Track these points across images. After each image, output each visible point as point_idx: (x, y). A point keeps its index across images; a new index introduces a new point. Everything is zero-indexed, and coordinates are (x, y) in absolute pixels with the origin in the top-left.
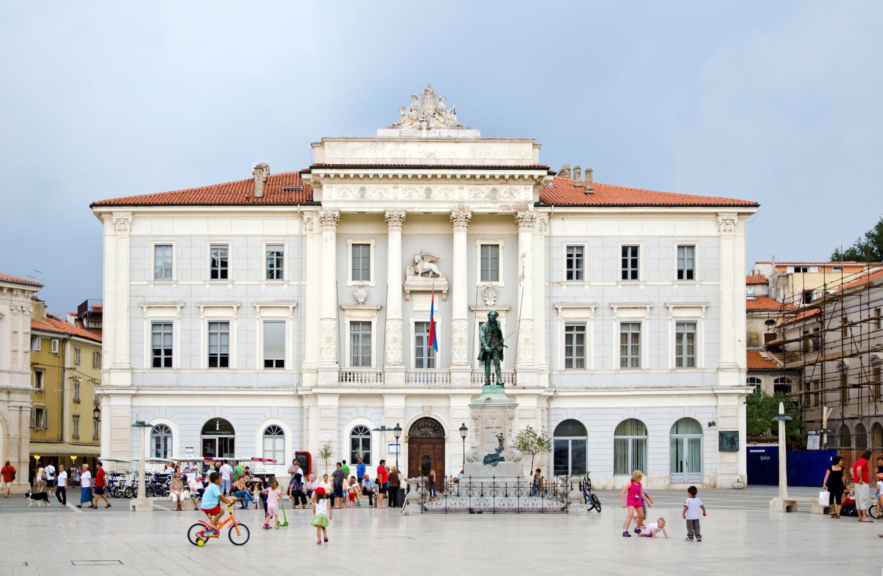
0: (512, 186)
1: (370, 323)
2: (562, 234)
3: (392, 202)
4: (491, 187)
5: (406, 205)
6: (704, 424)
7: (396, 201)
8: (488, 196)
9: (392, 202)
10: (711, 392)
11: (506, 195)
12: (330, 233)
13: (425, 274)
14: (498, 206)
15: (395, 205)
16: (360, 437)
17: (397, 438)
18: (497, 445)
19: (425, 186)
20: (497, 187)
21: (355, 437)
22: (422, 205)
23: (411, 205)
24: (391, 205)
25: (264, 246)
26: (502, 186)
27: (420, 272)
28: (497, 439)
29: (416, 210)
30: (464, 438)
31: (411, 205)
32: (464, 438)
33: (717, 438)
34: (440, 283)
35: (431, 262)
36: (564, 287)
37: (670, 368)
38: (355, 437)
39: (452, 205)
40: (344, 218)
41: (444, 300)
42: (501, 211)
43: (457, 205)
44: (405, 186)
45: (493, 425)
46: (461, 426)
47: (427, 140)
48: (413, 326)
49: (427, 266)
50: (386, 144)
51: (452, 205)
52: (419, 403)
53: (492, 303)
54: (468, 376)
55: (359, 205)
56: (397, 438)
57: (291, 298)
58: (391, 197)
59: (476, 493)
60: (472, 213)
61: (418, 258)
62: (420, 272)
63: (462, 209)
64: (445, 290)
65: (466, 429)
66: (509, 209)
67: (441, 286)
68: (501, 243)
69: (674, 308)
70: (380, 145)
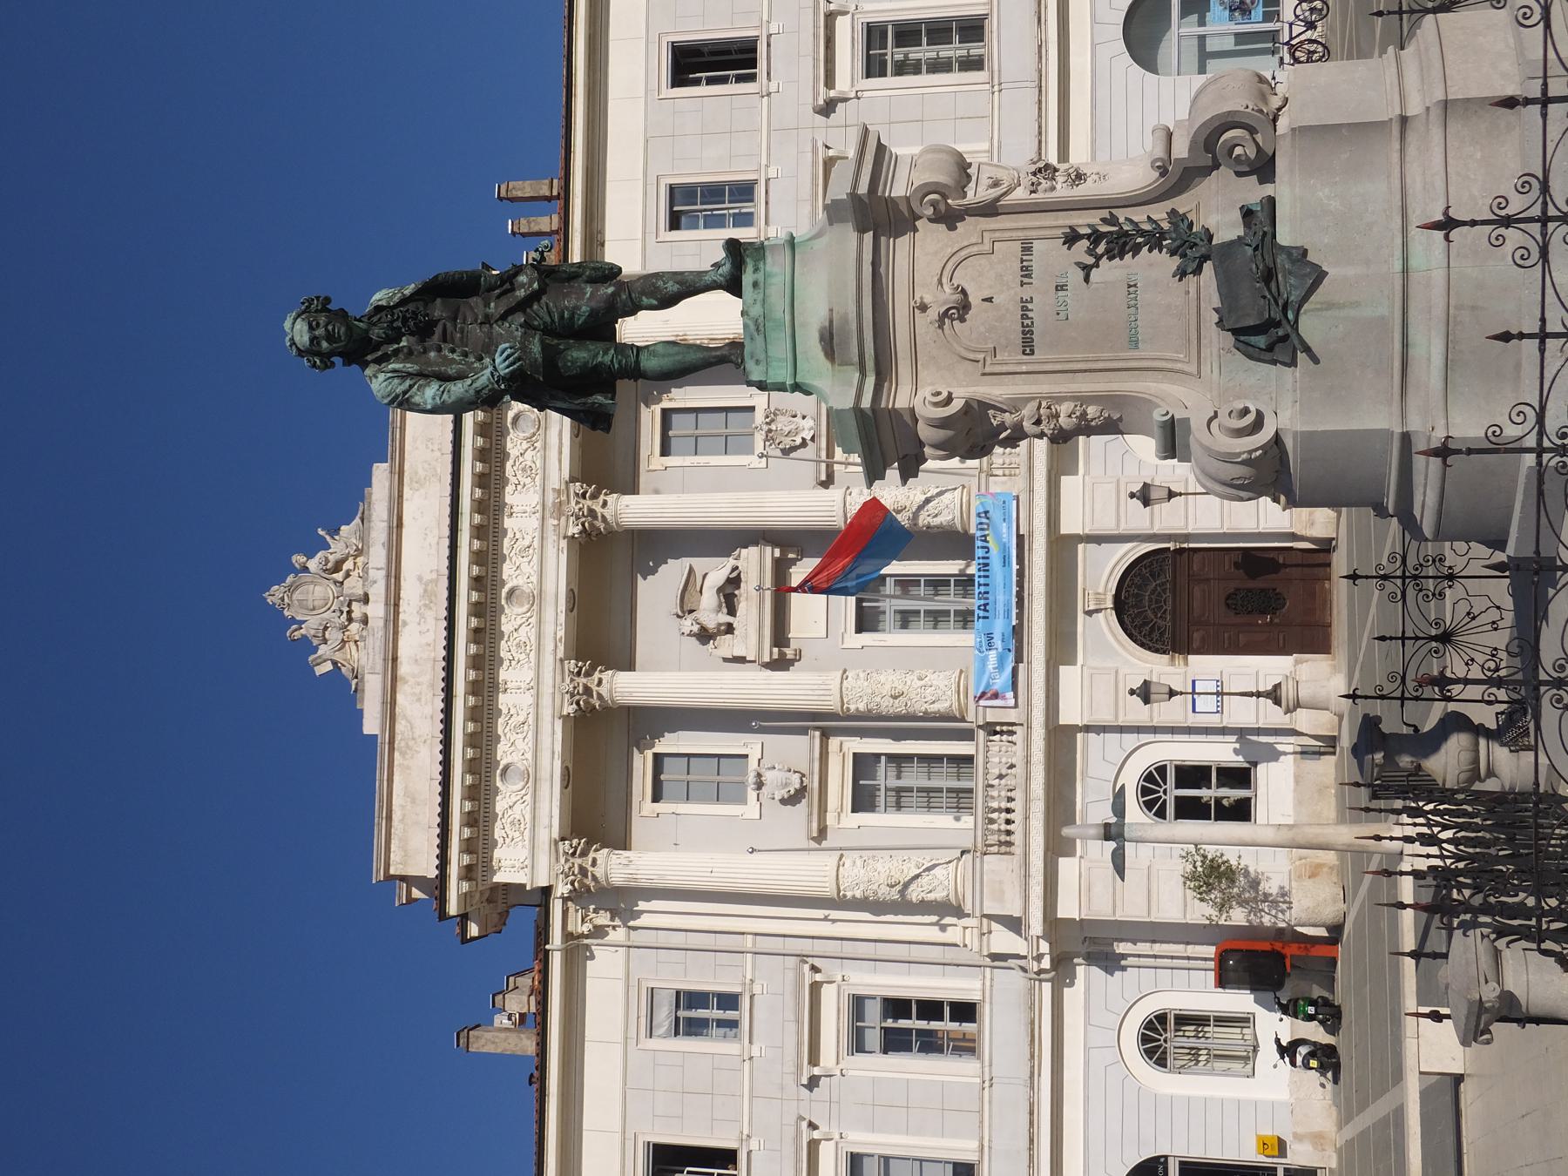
5: (548, 661)
15: (547, 688)
16: (1171, 792)
17: (1172, 693)
18: (1155, 266)
22: (549, 614)
23: (549, 646)
24: (546, 701)
25: (654, 1043)
27: (724, 618)
28: (1110, 271)
29: (561, 633)
30: (1171, 495)
31: (549, 646)
32: (1171, 495)
39: (551, 537)
45: (1007, 298)
46: (1137, 503)
48: (867, 638)
49: (709, 600)
51: (551, 537)
53: (809, 423)
55: (544, 789)
56: (1172, 693)
57: (790, 976)
58: (528, 699)
60: (573, 480)
61: (688, 625)
62: (724, 618)
63: (559, 509)
64: (770, 553)
65: (1146, 486)
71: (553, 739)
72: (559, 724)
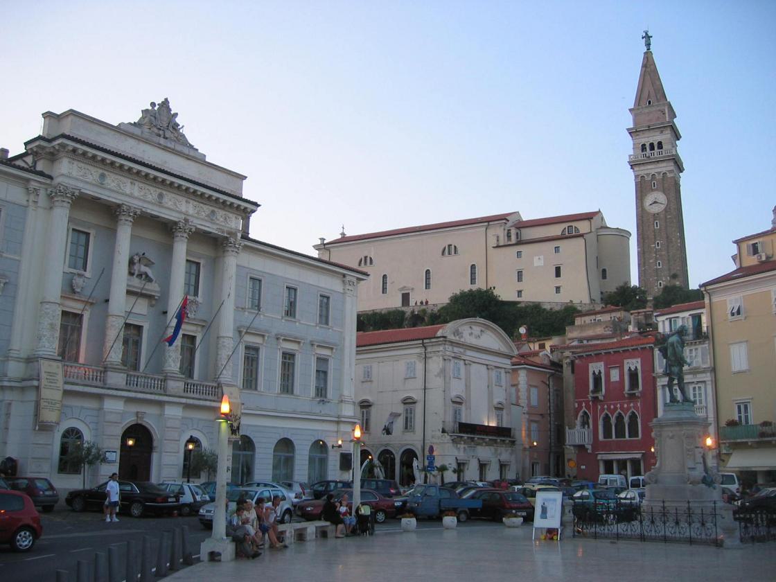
0: (227, 213)
1: (81, 316)
2: (246, 265)
3: (127, 195)
4: (211, 208)
5: (140, 204)
6: (329, 445)
7: (131, 196)
8: (207, 216)
9: (127, 195)
10: (336, 419)
11: (221, 219)
12: (61, 214)
13: (140, 276)
14: (215, 227)
19: (159, 191)
20: (216, 210)
21: (66, 440)
23: (145, 205)
24: (127, 199)
26: (220, 210)
29: (149, 211)
31: (145, 205)
33: (338, 458)
34: (153, 288)
35: (145, 265)
36: (246, 313)
37: (311, 396)
38: (66, 440)
40: (82, 202)
41: (152, 306)
42: (217, 232)
43: (183, 216)
44: (141, 185)
47: (165, 149)
49: (144, 269)
50: (128, 138)
52: (134, 408)
54: (181, 385)
58: (128, 192)
59: (671, 519)
62: (136, 273)
63: (186, 221)
66: (223, 232)
67: (156, 292)
68: (202, 262)
69: (318, 346)
70: (123, 137)
71: (114, 198)
72: (120, 202)
